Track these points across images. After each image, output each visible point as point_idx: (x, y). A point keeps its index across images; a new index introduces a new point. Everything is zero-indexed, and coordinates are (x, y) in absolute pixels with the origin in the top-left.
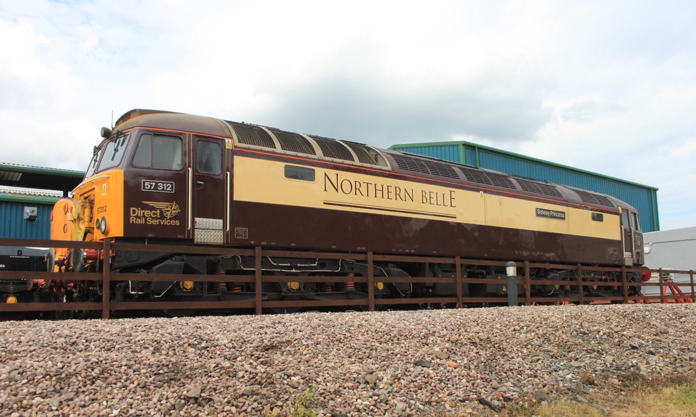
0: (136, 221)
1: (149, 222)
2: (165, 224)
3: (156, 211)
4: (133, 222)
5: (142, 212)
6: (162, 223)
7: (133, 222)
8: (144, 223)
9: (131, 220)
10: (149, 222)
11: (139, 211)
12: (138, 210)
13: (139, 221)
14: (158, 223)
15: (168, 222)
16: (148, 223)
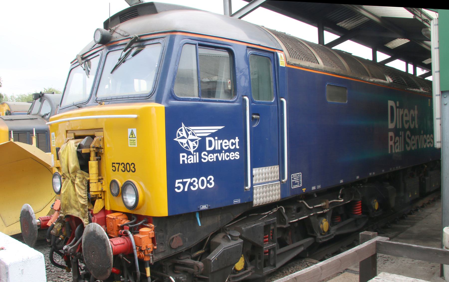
0: (187, 159)
1: (205, 159)
2: (224, 159)
3: (235, 139)
4: (184, 161)
5: (220, 142)
6: (220, 159)
7: (184, 161)
8: (198, 161)
9: (181, 159)
10: (205, 159)
11: (216, 141)
12: (215, 140)
13: (192, 159)
14: (215, 160)
15: (228, 156)
16: (202, 160)
